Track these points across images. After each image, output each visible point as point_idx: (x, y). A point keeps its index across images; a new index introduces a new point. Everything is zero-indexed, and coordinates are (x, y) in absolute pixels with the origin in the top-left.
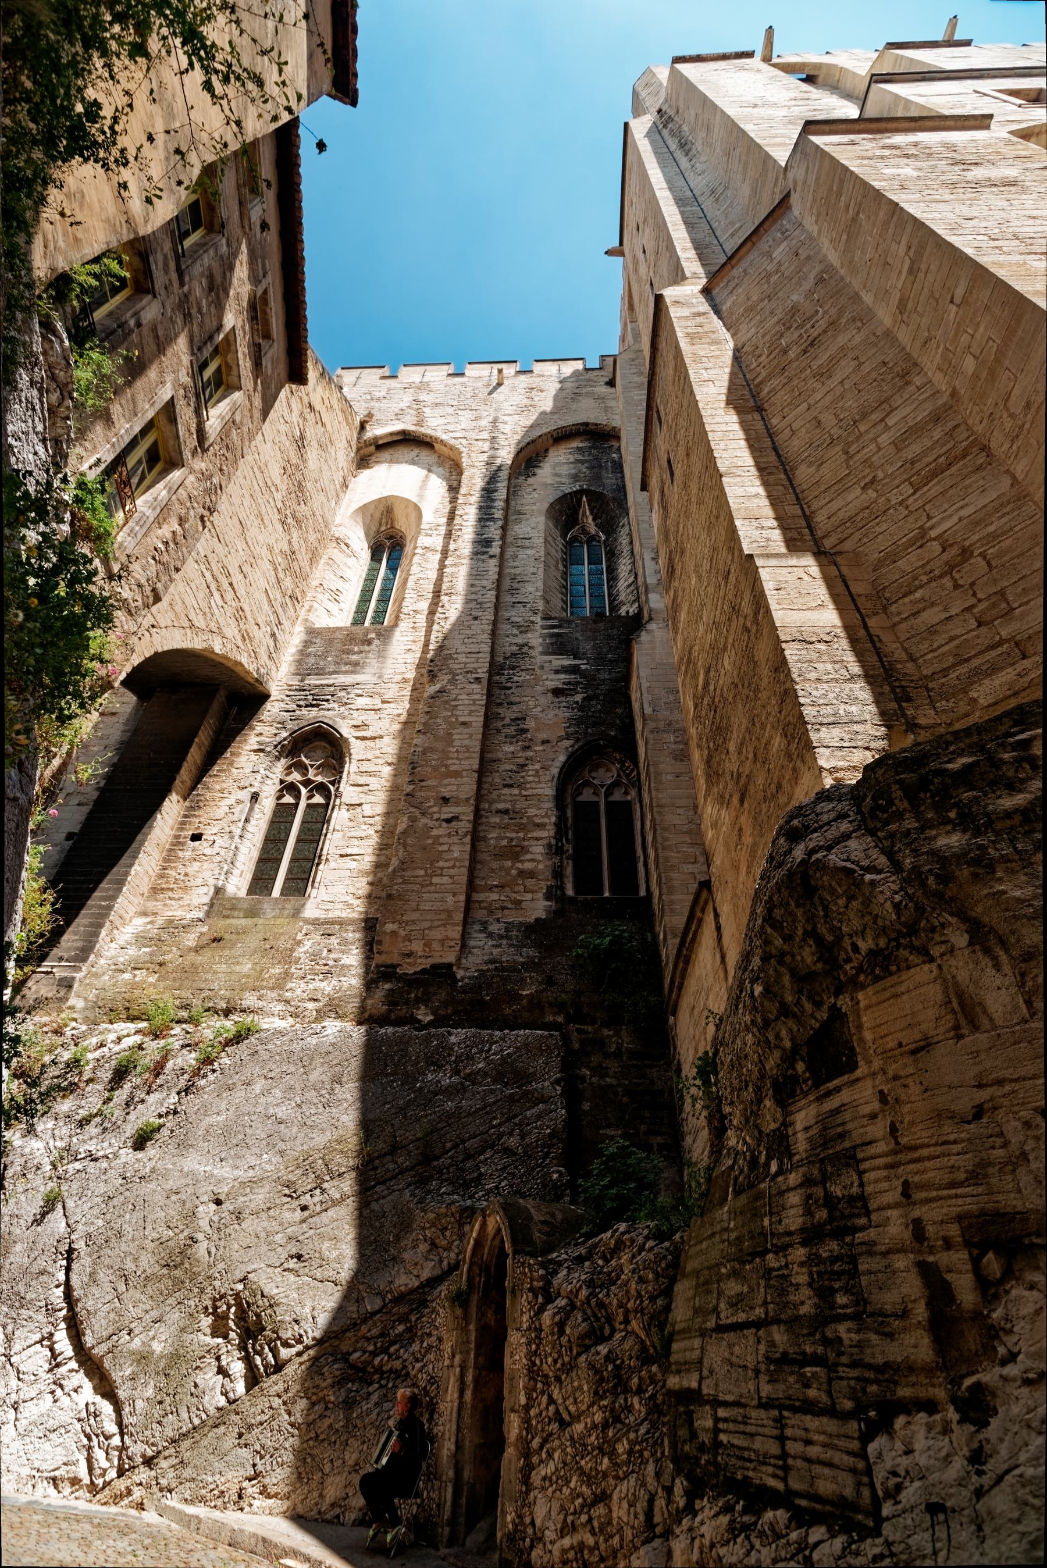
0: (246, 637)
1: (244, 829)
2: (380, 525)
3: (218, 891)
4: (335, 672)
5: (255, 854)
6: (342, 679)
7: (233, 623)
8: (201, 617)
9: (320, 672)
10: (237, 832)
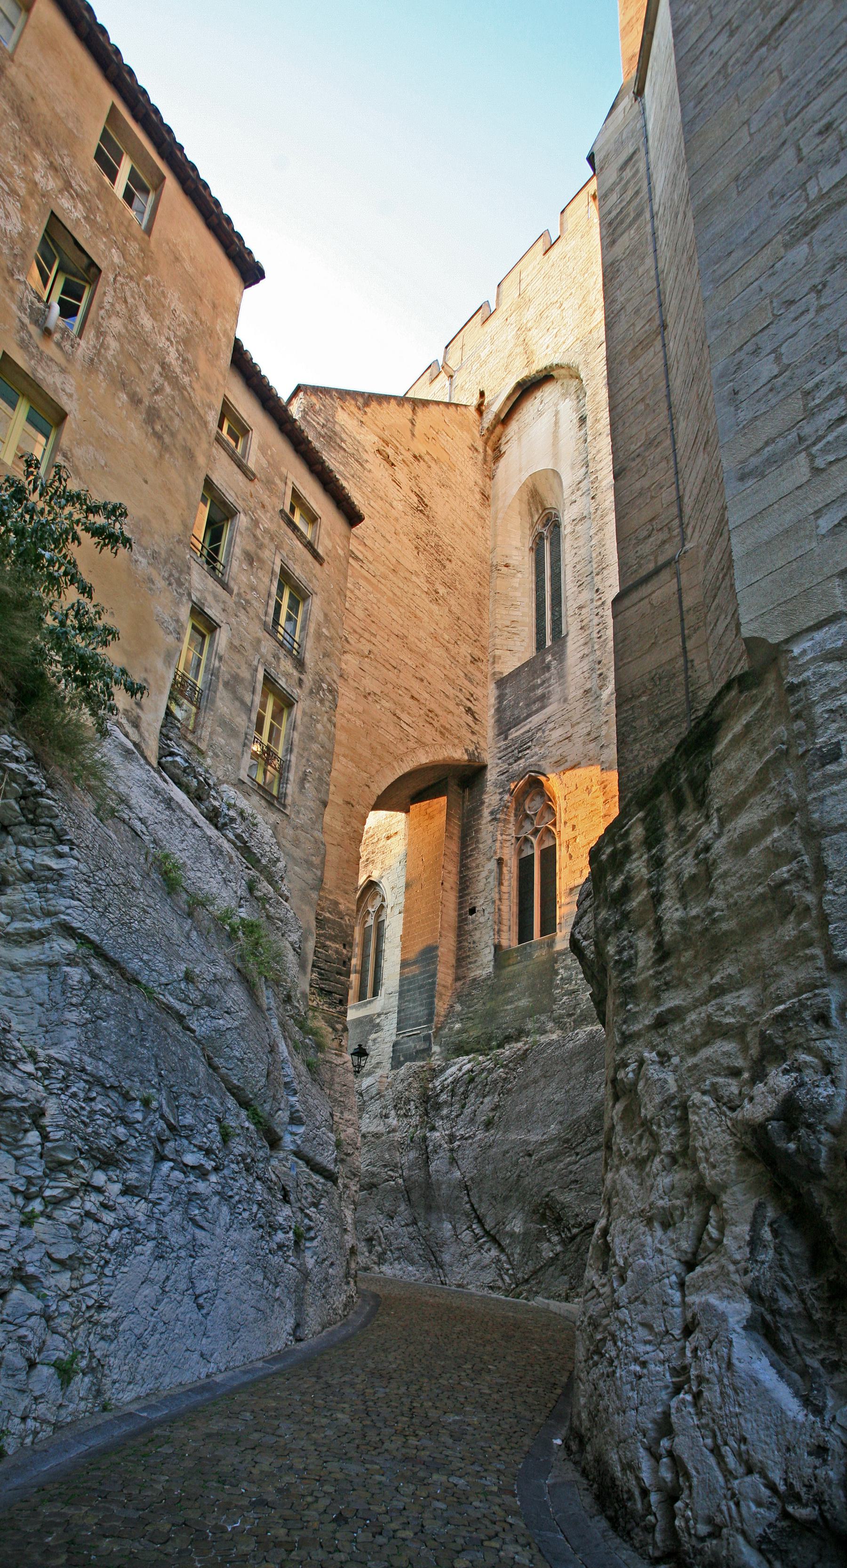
0: (443, 732)
1: (500, 892)
2: (532, 516)
3: (498, 947)
4: (529, 716)
5: (515, 909)
6: (536, 720)
7: (428, 729)
8: (400, 745)
9: (517, 722)
10: (497, 896)
